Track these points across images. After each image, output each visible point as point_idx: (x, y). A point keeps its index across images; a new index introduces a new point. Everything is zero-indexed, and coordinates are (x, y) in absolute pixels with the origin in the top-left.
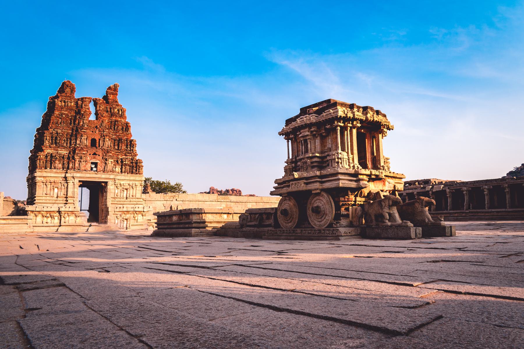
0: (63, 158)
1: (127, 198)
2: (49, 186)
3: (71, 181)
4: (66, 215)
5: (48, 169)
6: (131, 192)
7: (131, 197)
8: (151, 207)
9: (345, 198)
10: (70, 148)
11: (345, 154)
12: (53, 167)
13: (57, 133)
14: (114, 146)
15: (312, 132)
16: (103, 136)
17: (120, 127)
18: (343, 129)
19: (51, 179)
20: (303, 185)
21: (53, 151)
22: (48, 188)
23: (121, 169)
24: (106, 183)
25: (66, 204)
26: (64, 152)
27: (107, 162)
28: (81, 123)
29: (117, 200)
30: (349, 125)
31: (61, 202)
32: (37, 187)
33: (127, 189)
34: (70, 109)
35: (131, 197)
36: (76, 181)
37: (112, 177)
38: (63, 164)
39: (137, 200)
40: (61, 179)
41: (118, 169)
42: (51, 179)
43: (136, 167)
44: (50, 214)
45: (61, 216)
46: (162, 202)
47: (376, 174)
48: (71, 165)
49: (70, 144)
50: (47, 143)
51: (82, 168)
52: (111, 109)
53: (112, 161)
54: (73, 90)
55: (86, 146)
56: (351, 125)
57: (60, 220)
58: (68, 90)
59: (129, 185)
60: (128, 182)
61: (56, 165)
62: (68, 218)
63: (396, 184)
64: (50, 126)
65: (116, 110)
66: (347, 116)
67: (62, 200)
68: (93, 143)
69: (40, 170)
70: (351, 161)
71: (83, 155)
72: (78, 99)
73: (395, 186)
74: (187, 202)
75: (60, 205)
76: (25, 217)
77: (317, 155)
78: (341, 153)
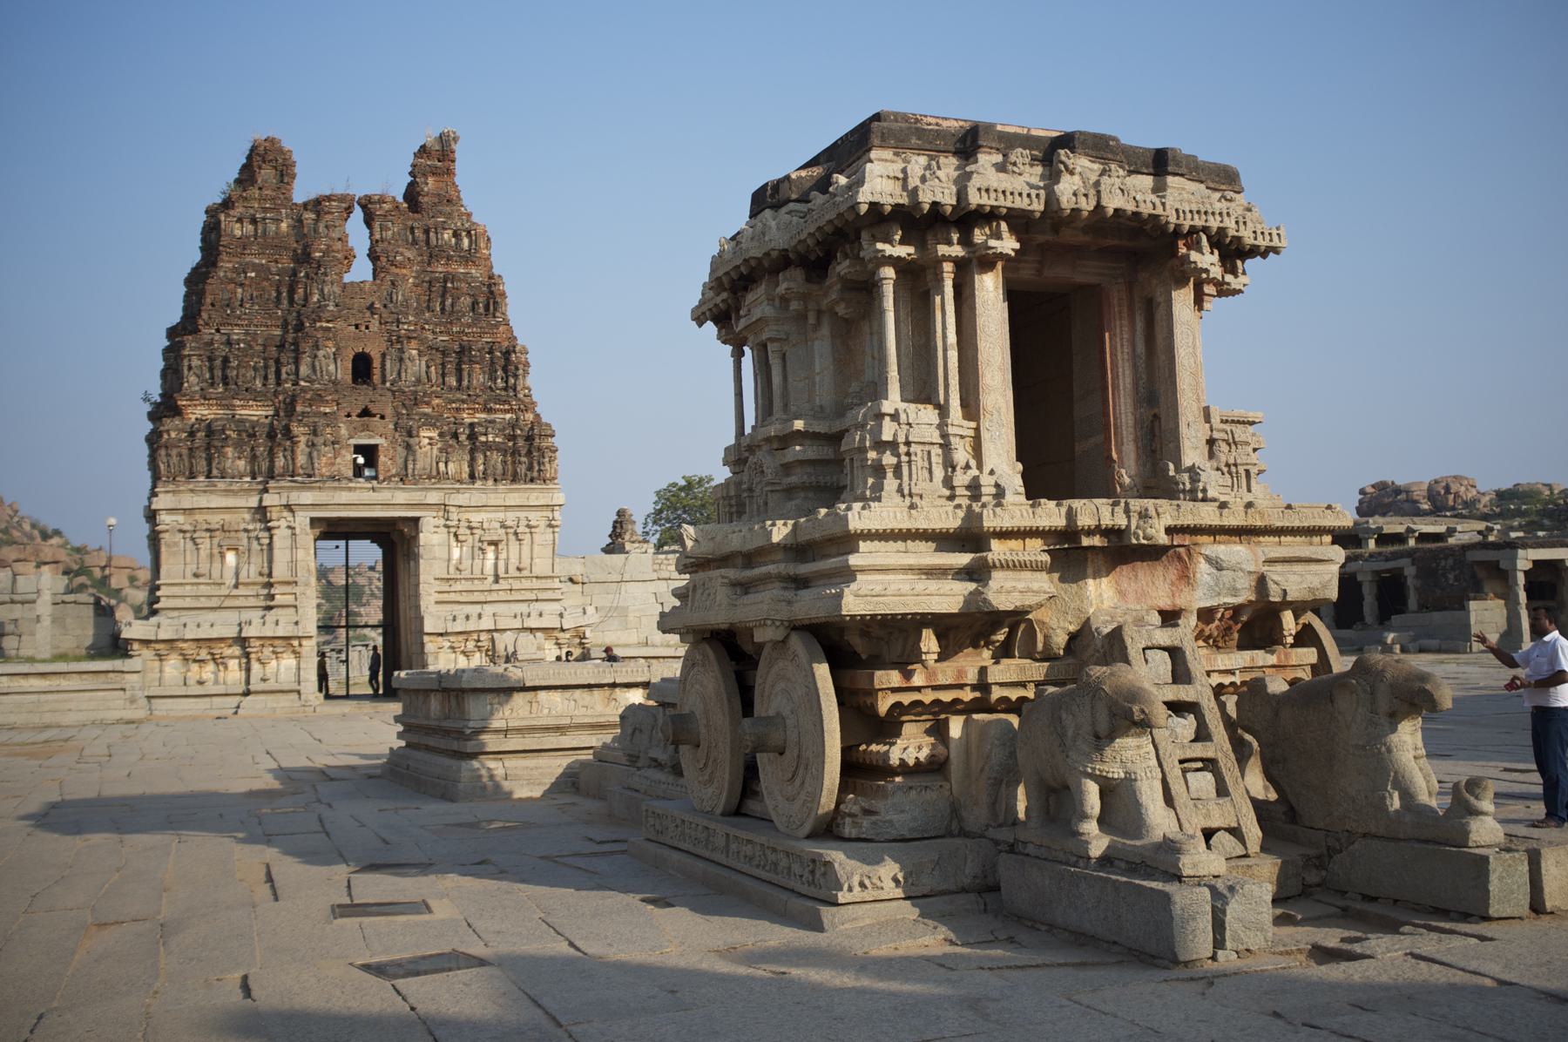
1: (497, 579)
3: (283, 523)
4: (268, 651)
5: (201, 479)
6: (512, 552)
7: (513, 572)
8: (590, 610)
9: (908, 675)
10: (276, 394)
11: (927, 415)
12: (215, 472)
13: (229, 343)
14: (443, 375)
15: (785, 300)
16: (397, 341)
17: (466, 301)
18: (917, 282)
19: (209, 518)
20: (722, 594)
21: (215, 410)
22: (204, 553)
25: (269, 608)
26: (256, 412)
27: (412, 441)
28: (315, 298)
29: (458, 586)
30: (943, 250)
31: (252, 602)
33: (495, 543)
35: (513, 572)
36: (302, 520)
37: (433, 497)
38: (254, 458)
39: (536, 584)
41: (457, 466)
43: (529, 453)
45: (247, 655)
46: (651, 587)
47: (1107, 521)
48: (280, 462)
49: (279, 382)
50: (191, 382)
51: (322, 466)
52: (427, 232)
53: (434, 434)
54: (285, 172)
55: (335, 383)
56: (957, 251)
57: (248, 670)
58: (266, 174)
59: (503, 526)
60: (501, 516)
62: (274, 663)
63: (1276, 574)
64: (205, 315)
65: (447, 235)
66: (917, 204)
67: (251, 595)
68: (362, 368)
69: (171, 487)
70: (962, 455)
71: (322, 421)
72: (305, 205)
73: (1261, 582)
75: (246, 615)
76: (117, 664)
77: (799, 425)
78: (895, 417)
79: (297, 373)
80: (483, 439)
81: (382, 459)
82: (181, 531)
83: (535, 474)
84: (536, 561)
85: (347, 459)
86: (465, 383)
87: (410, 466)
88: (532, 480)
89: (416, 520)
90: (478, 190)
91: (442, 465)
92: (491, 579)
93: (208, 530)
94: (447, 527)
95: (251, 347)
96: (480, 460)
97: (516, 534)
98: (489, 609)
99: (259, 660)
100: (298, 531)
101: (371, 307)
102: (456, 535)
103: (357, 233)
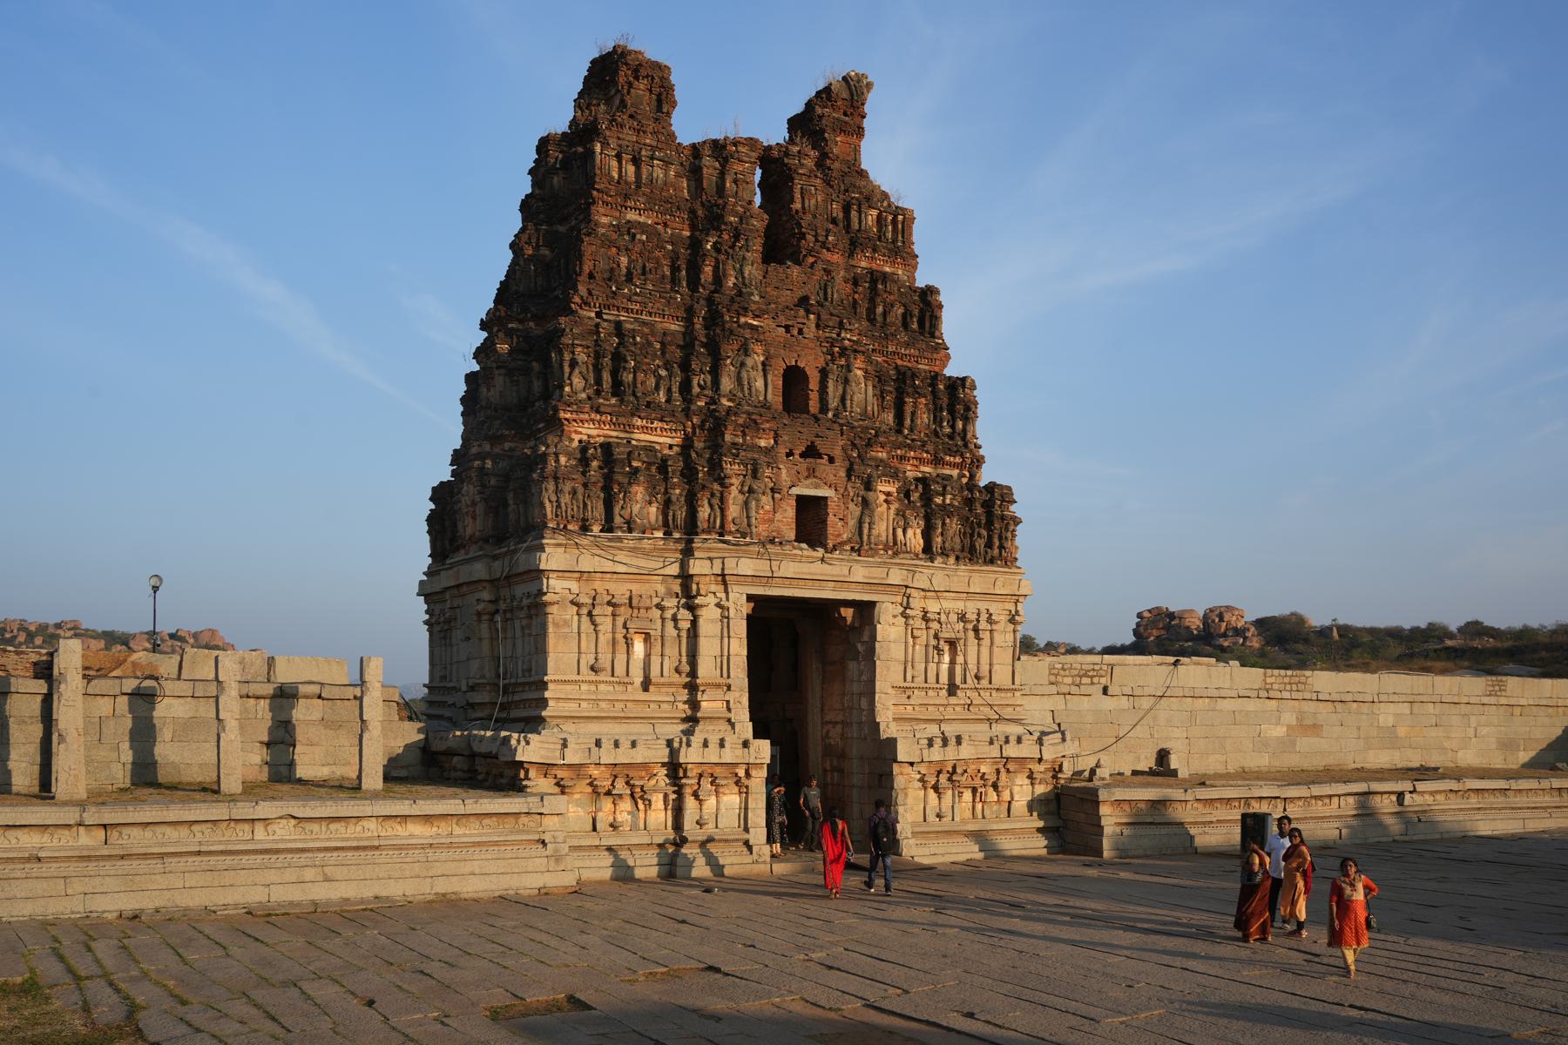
0: (663, 467)
2: (605, 624)
3: (711, 600)
4: (706, 784)
12: (618, 520)
22: (604, 638)
24: (866, 610)
32: (551, 629)
33: (952, 644)
34: (658, 199)
37: (896, 577)
38: (667, 503)
39: (997, 698)
40: (661, 589)
42: (612, 587)
43: (989, 525)
44: (627, 783)
48: (704, 512)
60: (960, 606)
79: (716, 384)
80: (939, 500)
82: (572, 602)
83: (996, 551)
84: (996, 668)
87: (866, 531)
88: (992, 561)
90: (888, 157)
91: (900, 532)
93: (609, 603)
94: (906, 617)
97: (976, 630)
99: (696, 795)
100: (732, 613)
101: (803, 301)
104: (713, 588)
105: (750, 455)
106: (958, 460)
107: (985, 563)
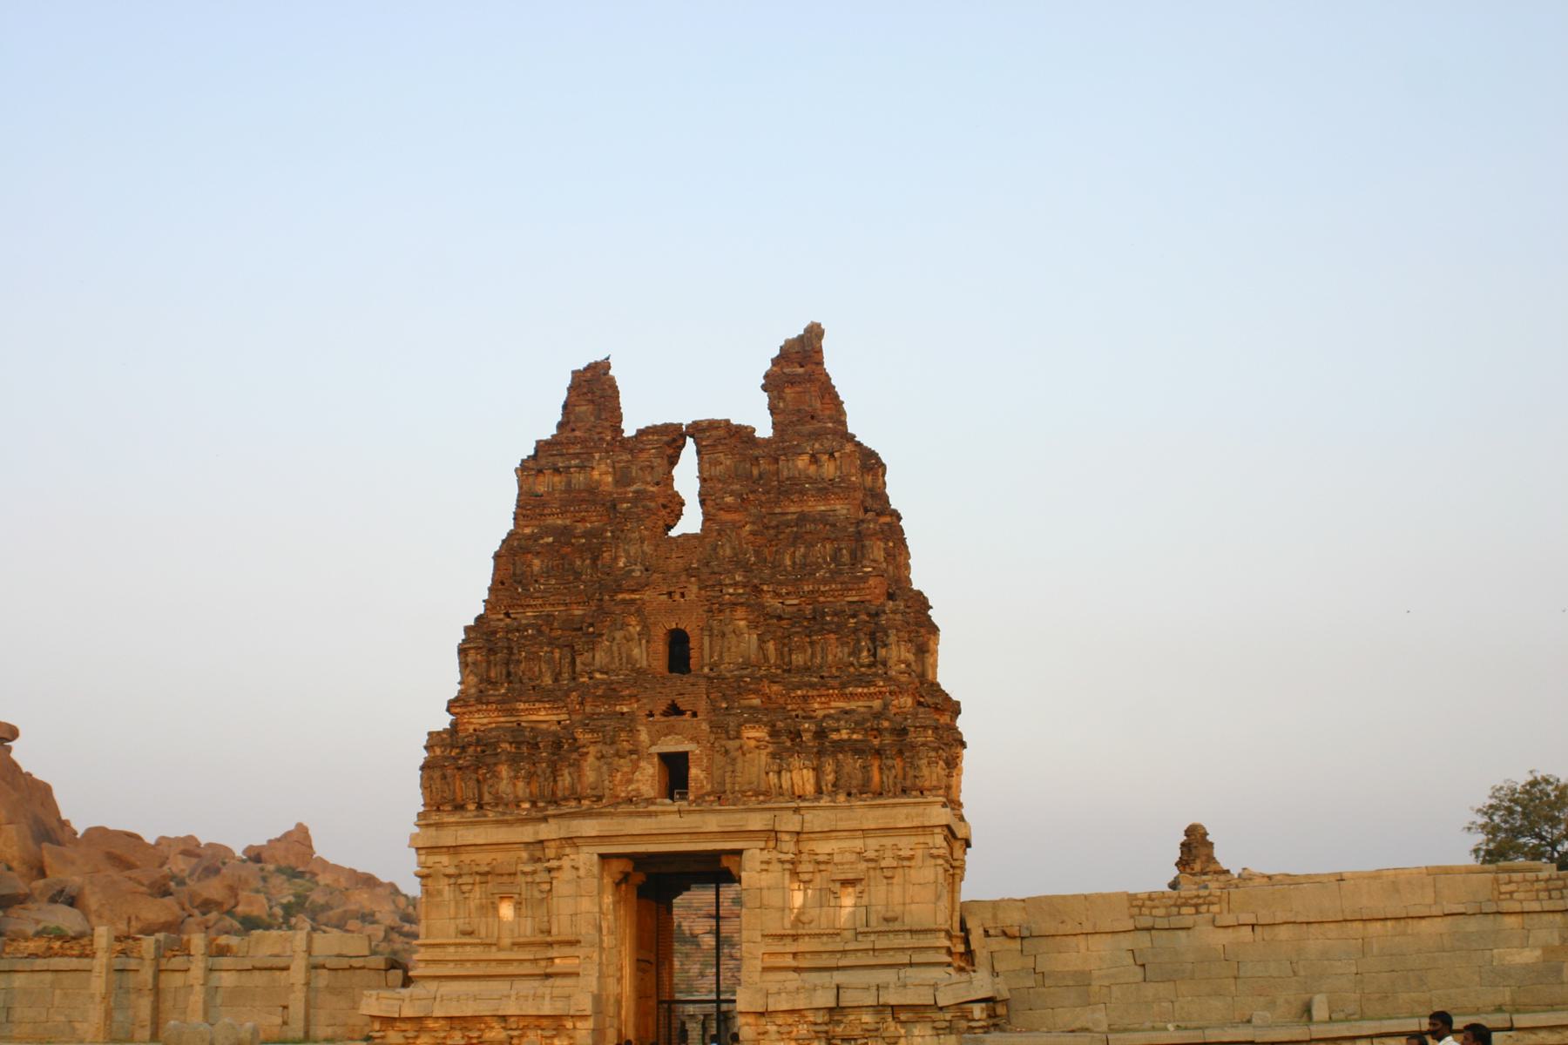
12: (487, 798)
19: (478, 857)
23: (818, 770)
26: (544, 717)
29: (802, 946)
36: (586, 858)
37: (757, 822)
39: (907, 941)
40: (525, 855)
46: (1127, 942)
48: (566, 779)
61: (504, 787)
65: (802, 462)
68: (678, 650)
69: (435, 818)
74: (1283, 933)
81: (694, 772)
85: (648, 777)
86: (818, 660)
87: (728, 780)
88: (904, 791)
89: (739, 852)
91: (773, 777)
92: (849, 934)
95: (540, 632)
96: (829, 767)
98: (839, 977)
100: (582, 873)
102: (795, 874)
103: (686, 476)
104: (568, 850)
105: (599, 723)
106: (872, 689)
107: (895, 796)
